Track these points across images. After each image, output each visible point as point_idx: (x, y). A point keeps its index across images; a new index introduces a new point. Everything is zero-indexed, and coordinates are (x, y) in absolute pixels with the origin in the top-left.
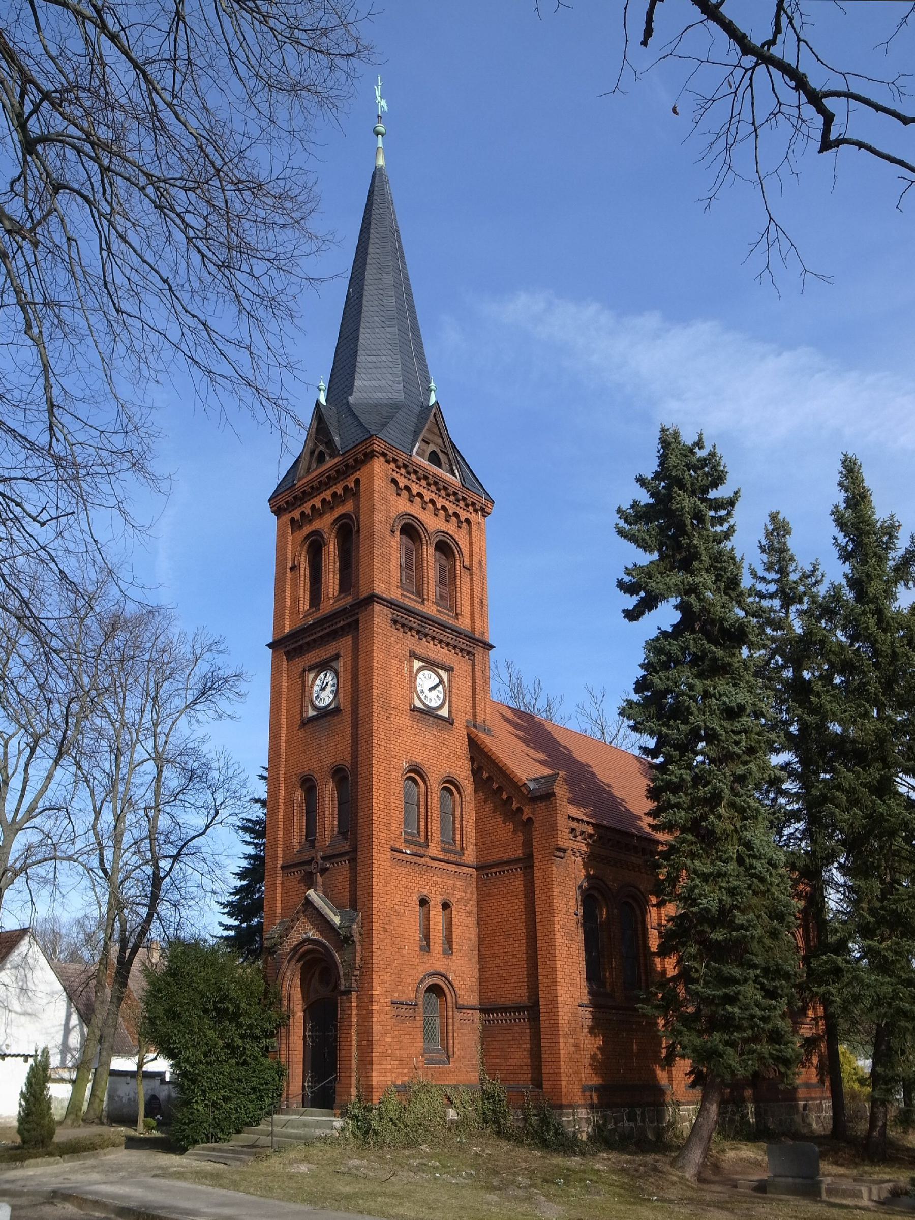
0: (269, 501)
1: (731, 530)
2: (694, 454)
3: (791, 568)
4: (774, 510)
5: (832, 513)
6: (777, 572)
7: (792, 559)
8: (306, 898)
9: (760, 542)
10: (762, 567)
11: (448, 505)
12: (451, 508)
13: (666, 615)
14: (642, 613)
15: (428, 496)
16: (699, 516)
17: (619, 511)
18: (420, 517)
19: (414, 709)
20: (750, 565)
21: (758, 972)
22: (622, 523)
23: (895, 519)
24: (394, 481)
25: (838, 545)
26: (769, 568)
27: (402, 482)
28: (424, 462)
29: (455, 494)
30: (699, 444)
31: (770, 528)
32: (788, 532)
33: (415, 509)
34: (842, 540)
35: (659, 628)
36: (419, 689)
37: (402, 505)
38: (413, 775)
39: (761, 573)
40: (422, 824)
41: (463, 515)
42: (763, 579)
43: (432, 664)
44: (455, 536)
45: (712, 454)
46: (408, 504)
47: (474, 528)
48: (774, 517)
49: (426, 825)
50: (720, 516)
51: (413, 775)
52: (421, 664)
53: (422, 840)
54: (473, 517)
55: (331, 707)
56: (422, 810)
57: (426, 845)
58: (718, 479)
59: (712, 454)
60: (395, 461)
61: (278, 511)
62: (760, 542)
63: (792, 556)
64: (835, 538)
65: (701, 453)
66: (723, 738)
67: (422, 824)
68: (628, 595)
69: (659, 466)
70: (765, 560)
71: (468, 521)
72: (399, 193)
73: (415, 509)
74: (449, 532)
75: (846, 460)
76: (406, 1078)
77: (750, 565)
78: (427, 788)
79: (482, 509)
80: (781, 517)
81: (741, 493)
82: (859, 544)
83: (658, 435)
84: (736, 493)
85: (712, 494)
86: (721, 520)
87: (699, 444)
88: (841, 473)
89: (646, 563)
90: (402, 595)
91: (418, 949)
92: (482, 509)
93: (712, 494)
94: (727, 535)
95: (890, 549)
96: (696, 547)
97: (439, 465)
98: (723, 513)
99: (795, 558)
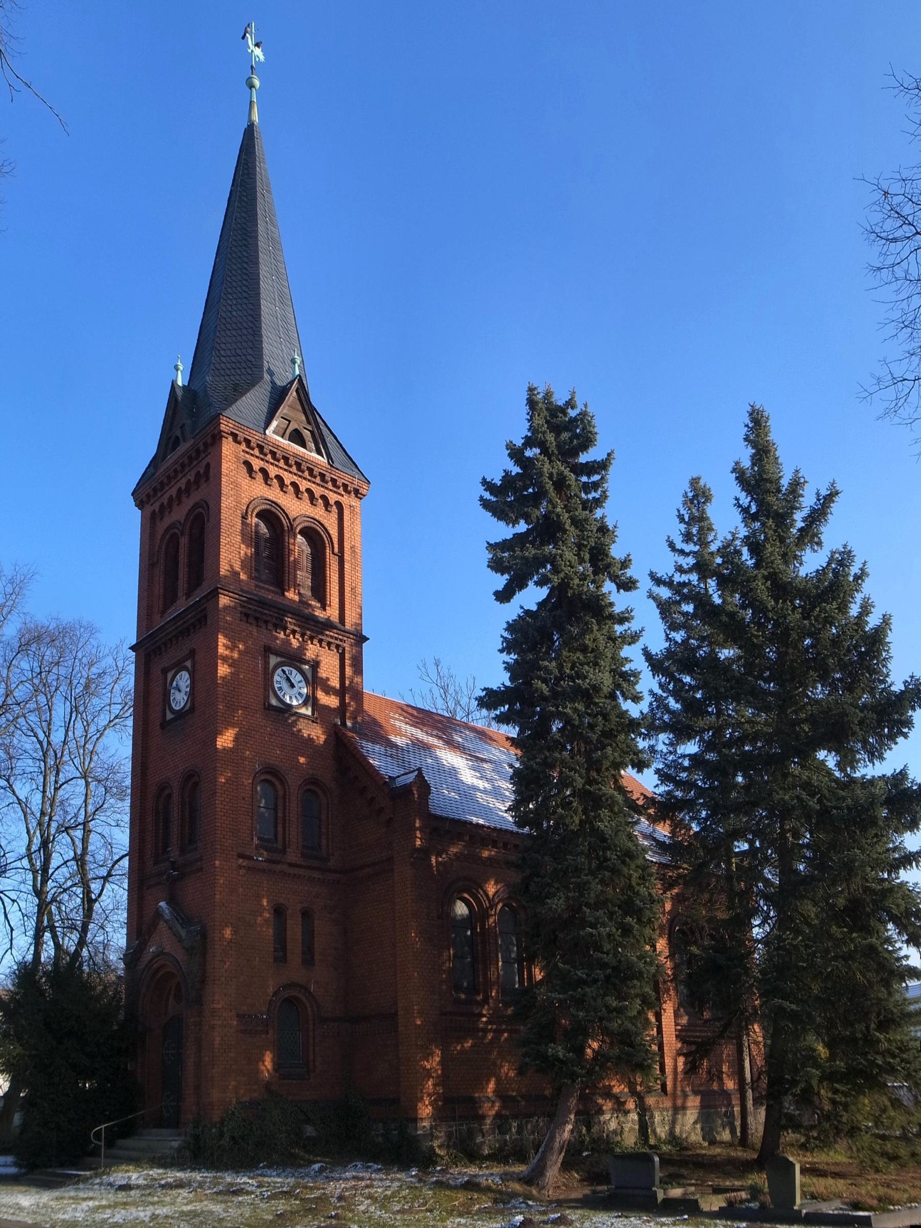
0: (132, 494)
1: (604, 496)
2: (565, 414)
3: (710, 538)
4: (694, 476)
5: (734, 470)
6: (695, 544)
7: (710, 529)
8: (157, 910)
9: (679, 511)
10: (681, 538)
11: (313, 487)
12: (318, 491)
13: (532, 596)
14: (512, 594)
15: (288, 478)
16: (560, 484)
17: (484, 482)
18: (279, 501)
19: (270, 707)
20: (669, 537)
21: (609, 971)
22: (487, 495)
23: (800, 475)
24: (247, 464)
25: (740, 506)
26: (688, 537)
27: (257, 464)
28: (284, 442)
29: (322, 476)
30: (570, 404)
31: (690, 495)
32: (708, 499)
33: (274, 494)
34: (745, 500)
35: (522, 607)
36: (276, 686)
37: (257, 489)
38: (313, 788)
39: (679, 545)
40: (280, 829)
41: (333, 497)
42: (682, 552)
43: (292, 660)
44: (324, 522)
45: (584, 414)
46: (266, 488)
47: (346, 512)
48: (694, 482)
49: (284, 833)
50: (594, 482)
51: (313, 788)
52: (279, 659)
53: (280, 845)
54: (346, 500)
55: (186, 708)
56: (280, 815)
57: (284, 851)
58: (586, 441)
59: (584, 414)
60: (248, 442)
61: (140, 504)
62: (679, 511)
63: (711, 524)
64: (737, 499)
65: (572, 413)
66: (577, 723)
67: (280, 829)
68: (499, 575)
69: (529, 430)
70: (683, 530)
71: (339, 505)
72: (264, 146)
73: (274, 494)
74: (317, 517)
75: (753, 411)
76: (256, 1095)
77: (669, 537)
78: (285, 792)
79: (357, 492)
80: (702, 483)
81: (614, 455)
82: (761, 503)
83: (525, 396)
84: (609, 455)
85: (583, 458)
86: (596, 486)
87: (570, 404)
88: (747, 426)
89: (509, 536)
90: (257, 586)
91: (271, 960)
92: (357, 492)
93: (583, 458)
94: (598, 502)
95: (797, 508)
96: (558, 516)
97: (303, 444)
98: (596, 478)
99: (714, 527)
